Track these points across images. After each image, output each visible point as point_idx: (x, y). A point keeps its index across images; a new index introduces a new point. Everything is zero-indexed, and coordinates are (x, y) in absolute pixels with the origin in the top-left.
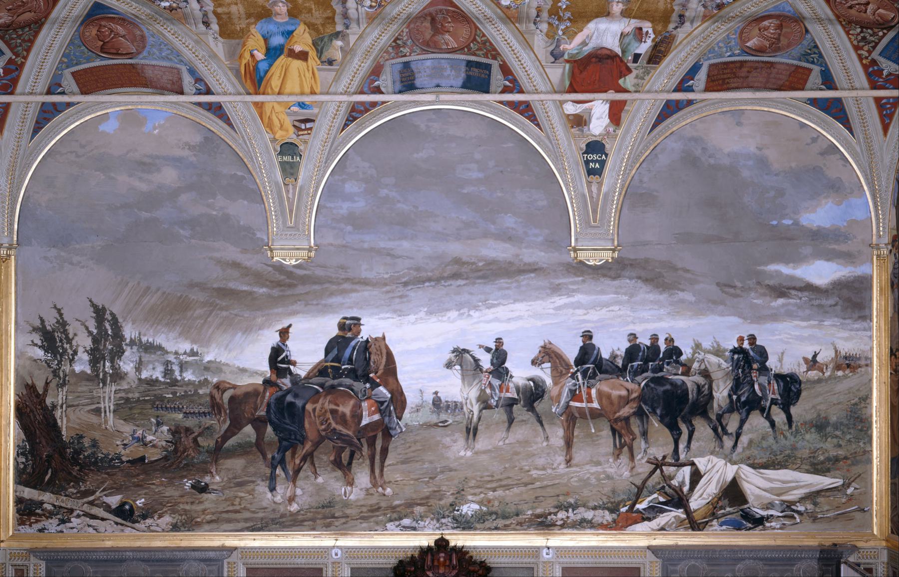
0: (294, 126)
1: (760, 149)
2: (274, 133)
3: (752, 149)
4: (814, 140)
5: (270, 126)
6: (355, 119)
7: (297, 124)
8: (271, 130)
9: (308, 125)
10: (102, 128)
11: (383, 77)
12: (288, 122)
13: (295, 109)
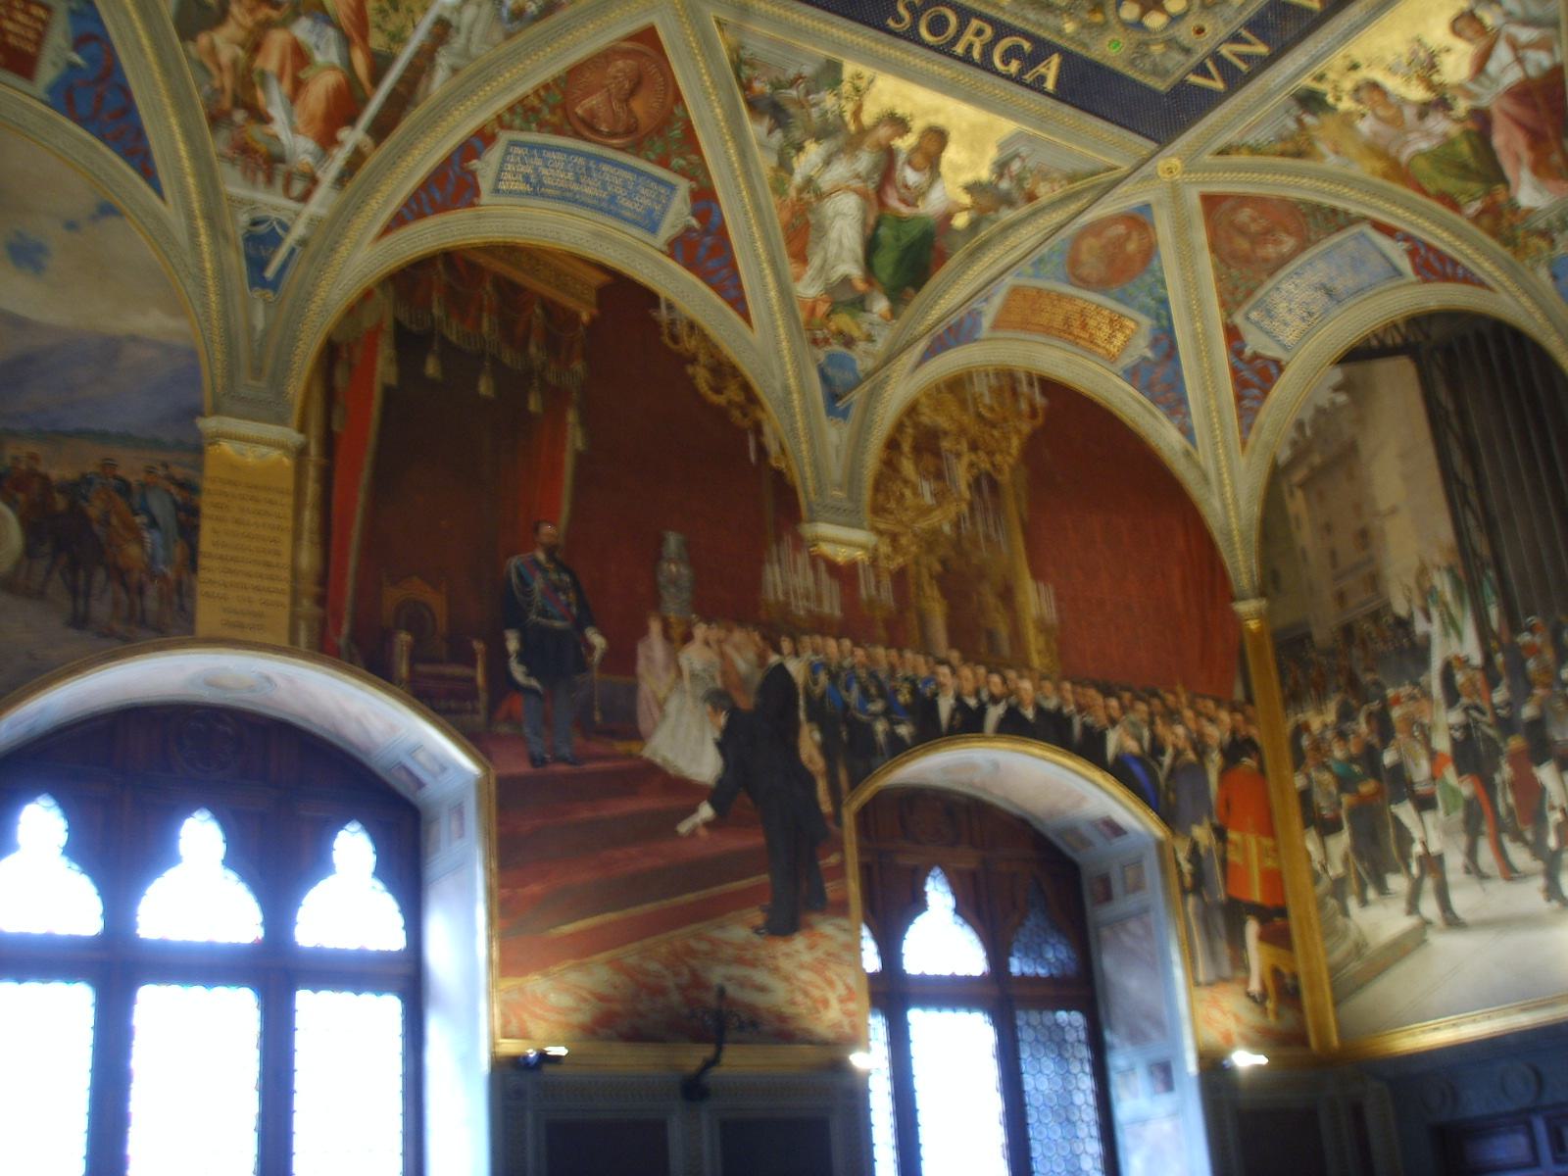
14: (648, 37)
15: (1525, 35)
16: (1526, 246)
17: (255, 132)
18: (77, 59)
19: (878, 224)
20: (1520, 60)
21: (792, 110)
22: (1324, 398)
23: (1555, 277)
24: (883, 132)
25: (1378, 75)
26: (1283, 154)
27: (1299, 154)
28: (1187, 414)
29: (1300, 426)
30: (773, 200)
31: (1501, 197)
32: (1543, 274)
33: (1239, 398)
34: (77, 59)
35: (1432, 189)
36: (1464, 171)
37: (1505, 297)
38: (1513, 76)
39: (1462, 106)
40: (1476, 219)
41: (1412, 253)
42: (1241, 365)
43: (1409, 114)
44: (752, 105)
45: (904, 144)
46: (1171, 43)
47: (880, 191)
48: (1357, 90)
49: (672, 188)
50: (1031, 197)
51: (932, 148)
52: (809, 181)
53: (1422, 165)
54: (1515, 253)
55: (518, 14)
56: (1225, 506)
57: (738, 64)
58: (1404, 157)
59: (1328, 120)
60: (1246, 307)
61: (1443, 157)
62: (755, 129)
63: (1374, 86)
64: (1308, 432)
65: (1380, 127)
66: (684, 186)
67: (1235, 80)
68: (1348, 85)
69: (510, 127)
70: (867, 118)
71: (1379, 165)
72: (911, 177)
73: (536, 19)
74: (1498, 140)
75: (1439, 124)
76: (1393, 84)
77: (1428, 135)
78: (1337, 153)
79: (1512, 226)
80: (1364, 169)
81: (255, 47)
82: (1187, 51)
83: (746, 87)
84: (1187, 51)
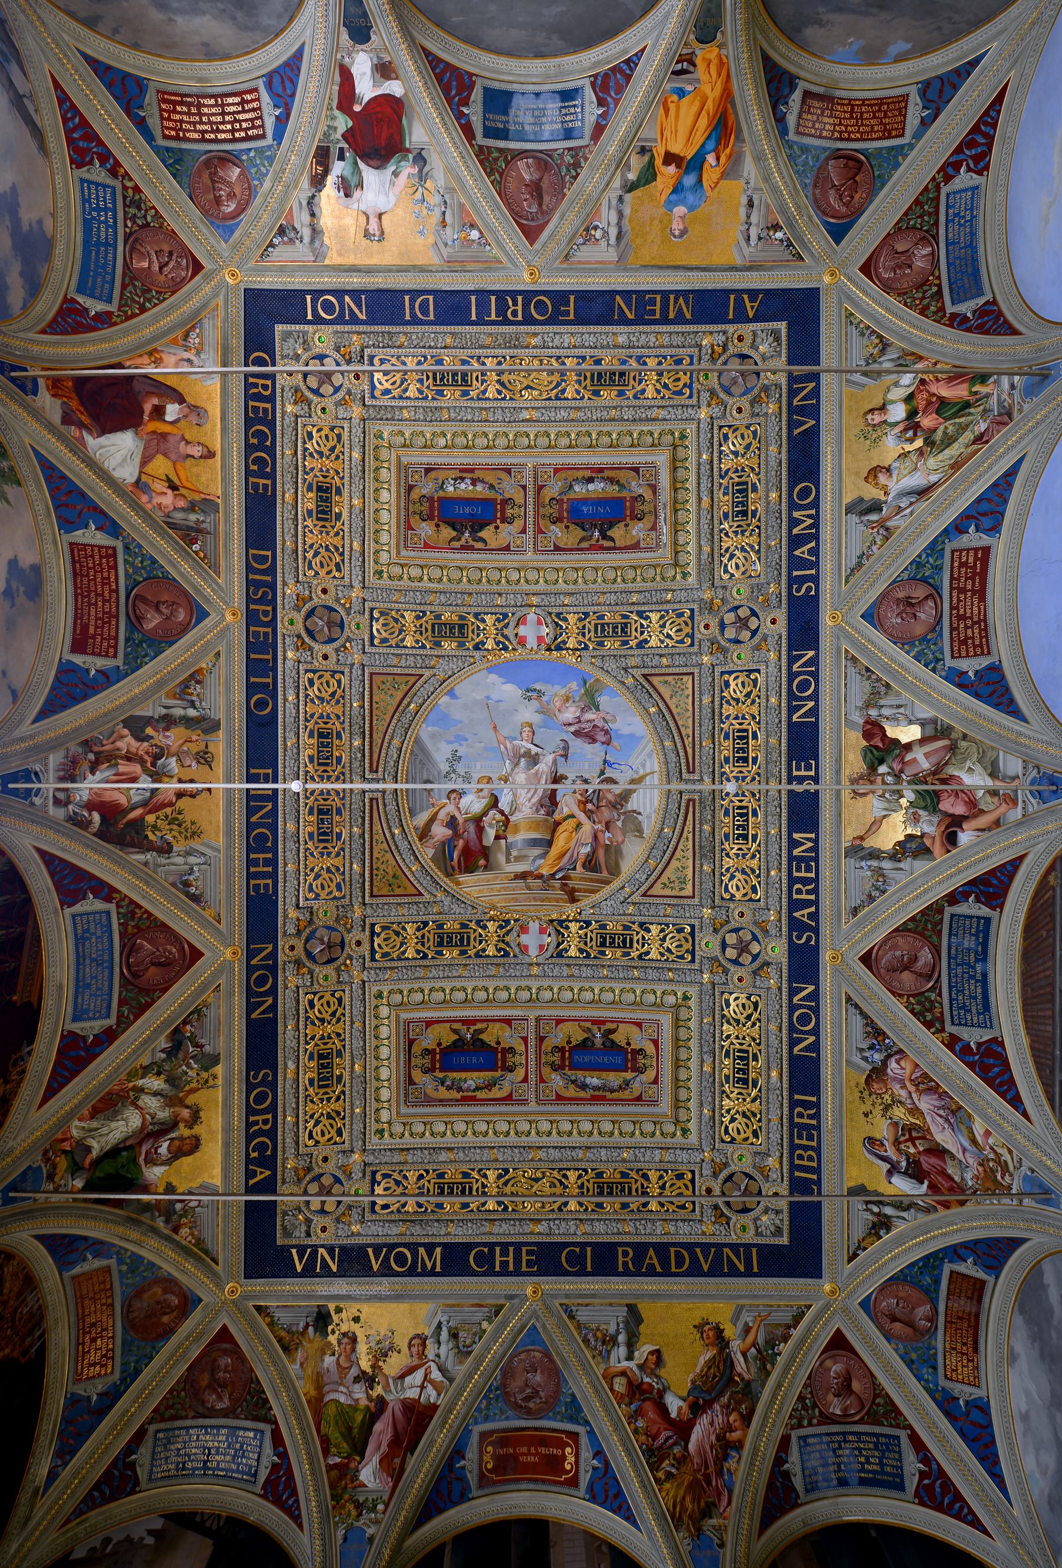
0: (695, 65)
1: (170, 19)
2: (719, 56)
3: (180, 20)
4: (116, 31)
5: (721, 64)
6: (627, 62)
7: (691, 69)
8: (721, 60)
9: (679, 67)
10: (909, 46)
11: (593, 118)
12: (701, 72)
13: (689, 88)
14: (196, 954)
15: (436, 1375)
16: (343, 1507)
17: (86, 766)
18: (93, 672)
19: (126, 1148)
20: (422, 1387)
21: (180, 1056)
22: (138, 1532)
23: (345, 1539)
24: (185, 1113)
25: (361, 1338)
26: (280, 1340)
27: (286, 1349)
28: (65, 1464)
29: (107, 1540)
30: (123, 1076)
31: (353, 1465)
32: (341, 1533)
33: (97, 1486)
34: (93, 672)
35: (323, 1432)
36: (347, 1433)
37: (305, 1539)
38: (412, 1394)
39: (378, 1390)
40: (330, 1468)
41: (275, 1467)
42: (120, 1464)
43: (354, 1372)
44: (176, 1030)
45: (183, 1131)
46: (308, 1221)
47: (149, 1135)
48: (345, 1334)
49: (108, 1016)
50: (176, 1230)
51: (186, 1148)
52: (142, 1090)
53: (332, 1410)
54: (334, 1507)
55: (187, 884)
56: (17, 1551)
57: (197, 1011)
58: (326, 1399)
59: (318, 1338)
60: (163, 1426)
61: (345, 1413)
62: (163, 1043)
63: (354, 1340)
64: (108, 1550)
65: (334, 1369)
66: (112, 1021)
67: (309, 1271)
68: (344, 1328)
69: (118, 906)
70: (191, 1100)
71: (313, 1393)
72: (163, 1149)
73: (188, 895)
74: (378, 1427)
75: (359, 1392)
76: (362, 1348)
77: (349, 1394)
78: (302, 1364)
79: (345, 1487)
80: (304, 1388)
81: (129, 758)
82: (308, 1235)
83: (185, 1022)
84: (308, 1235)
